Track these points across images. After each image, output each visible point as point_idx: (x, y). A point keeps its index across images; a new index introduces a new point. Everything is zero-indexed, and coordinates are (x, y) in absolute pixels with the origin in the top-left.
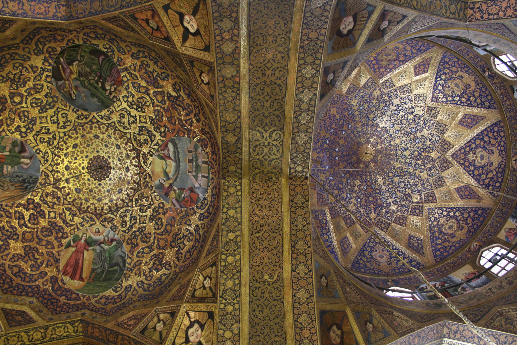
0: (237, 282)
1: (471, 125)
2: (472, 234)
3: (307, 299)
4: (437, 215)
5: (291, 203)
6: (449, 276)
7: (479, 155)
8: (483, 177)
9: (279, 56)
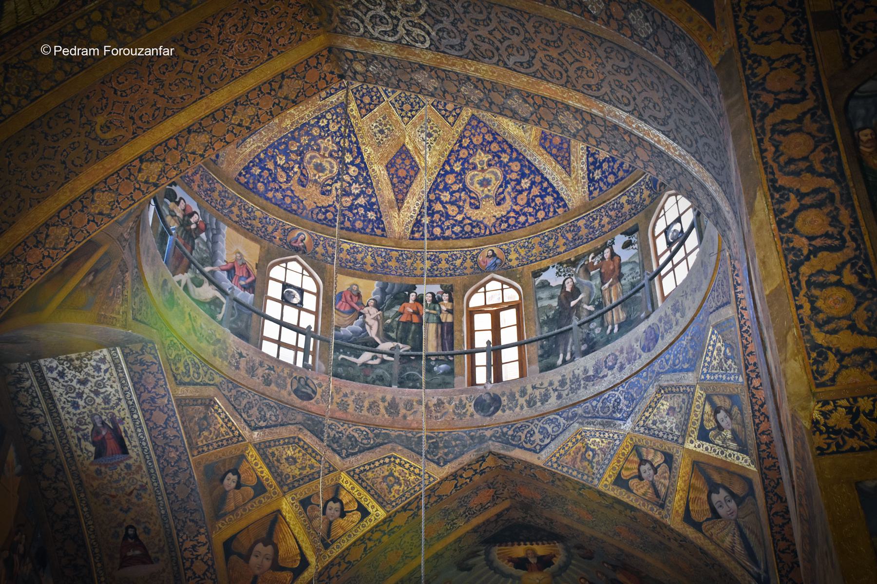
0: (59, 76)
1: (547, 145)
2: (324, 219)
3: (100, 213)
4: (333, 127)
5: (278, 79)
6: (222, 225)
7: (488, 176)
8: (446, 197)
9: (593, 82)
